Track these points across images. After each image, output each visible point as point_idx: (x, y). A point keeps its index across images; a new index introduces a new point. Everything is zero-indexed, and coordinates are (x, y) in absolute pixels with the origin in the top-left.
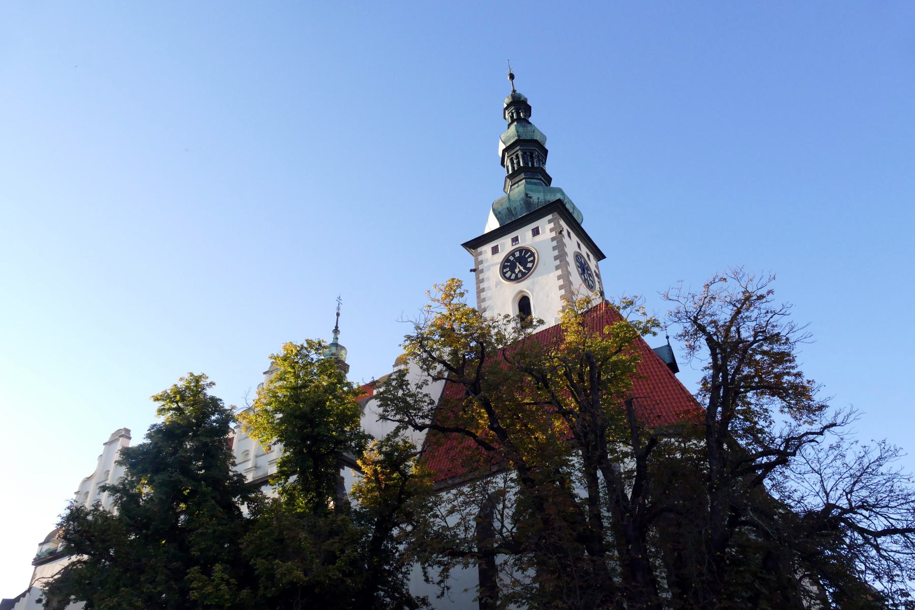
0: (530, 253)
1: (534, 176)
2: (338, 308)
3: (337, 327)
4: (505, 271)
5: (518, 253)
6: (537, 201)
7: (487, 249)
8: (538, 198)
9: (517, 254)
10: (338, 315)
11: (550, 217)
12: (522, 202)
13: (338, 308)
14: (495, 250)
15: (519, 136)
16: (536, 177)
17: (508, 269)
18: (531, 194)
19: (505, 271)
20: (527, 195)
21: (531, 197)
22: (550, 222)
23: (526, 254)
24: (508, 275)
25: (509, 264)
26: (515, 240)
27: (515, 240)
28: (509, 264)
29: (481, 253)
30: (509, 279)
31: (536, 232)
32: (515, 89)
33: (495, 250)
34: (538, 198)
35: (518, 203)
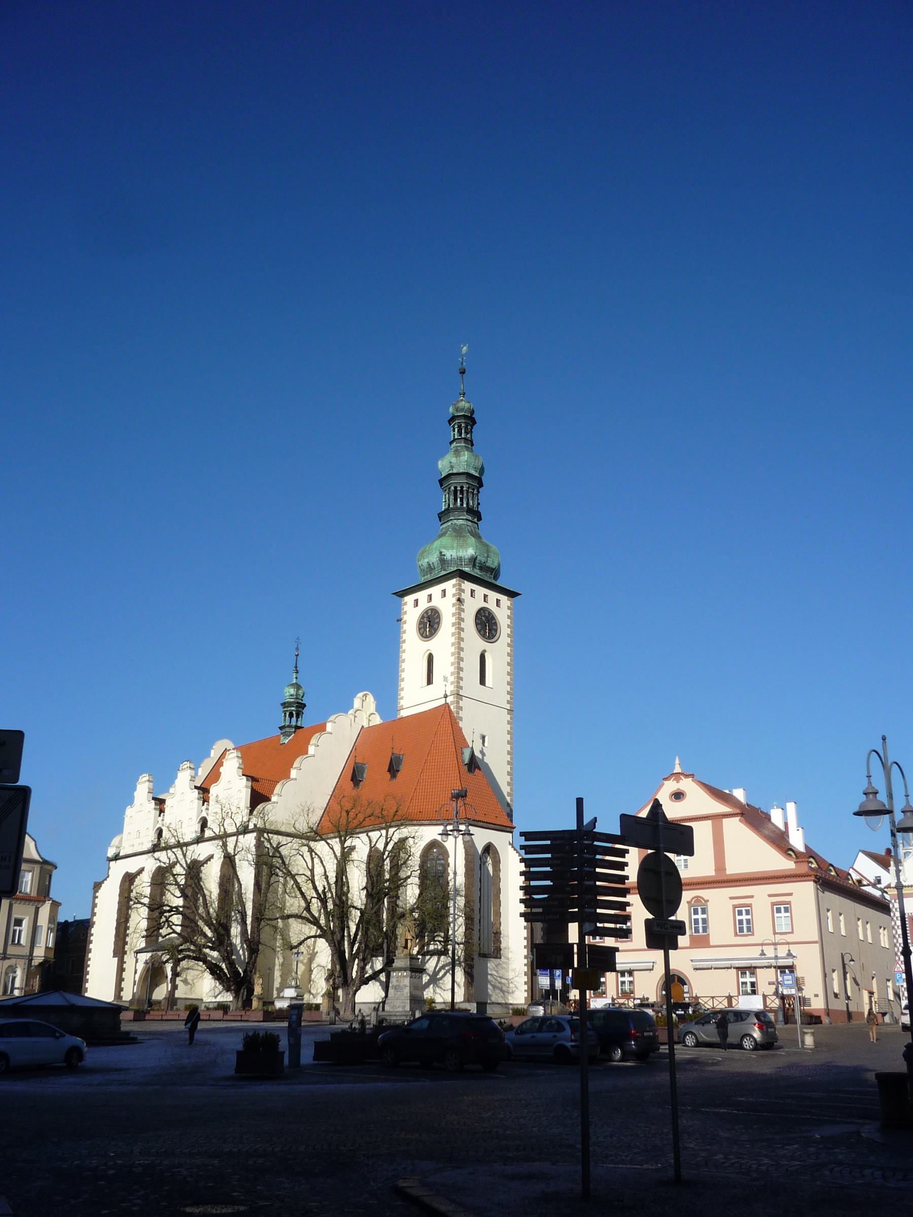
1: (461, 516)
2: (297, 649)
3: (296, 667)
6: (450, 558)
7: (409, 599)
8: (451, 556)
9: (430, 614)
10: (297, 655)
11: (454, 581)
12: (437, 559)
13: (297, 649)
15: (452, 467)
16: (461, 517)
18: (445, 552)
20: (441, 553)
21: (444, 555)
23: (434, 615)
33: (416, 602)
34: (451, 556)
35: (435, 560)
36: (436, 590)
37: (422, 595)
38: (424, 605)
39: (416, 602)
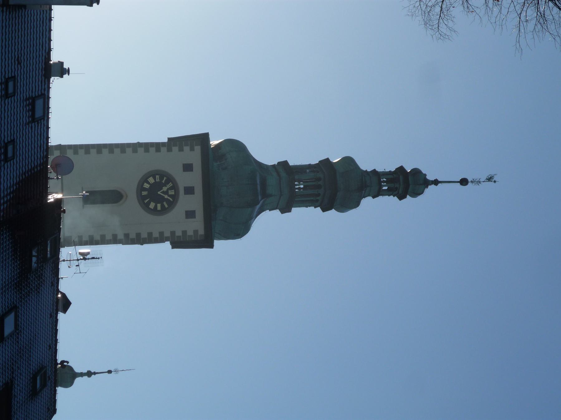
0: (166, 206)
4: (157, 177)
5: (173, 193)
9: (172, 192)
11: (201, 232)
14: (188, 168)
17: (158, 180)
19: (157, 177)
22: (196, 232)
24: (151, 180)
25: (163, 181)
26: (189, 191)
27: (189, 191)
28: (163, 181)
29: (192, 149)
30: (145, 179)
31: (190, 214)
32: (439, 184)
39: (188, 168)
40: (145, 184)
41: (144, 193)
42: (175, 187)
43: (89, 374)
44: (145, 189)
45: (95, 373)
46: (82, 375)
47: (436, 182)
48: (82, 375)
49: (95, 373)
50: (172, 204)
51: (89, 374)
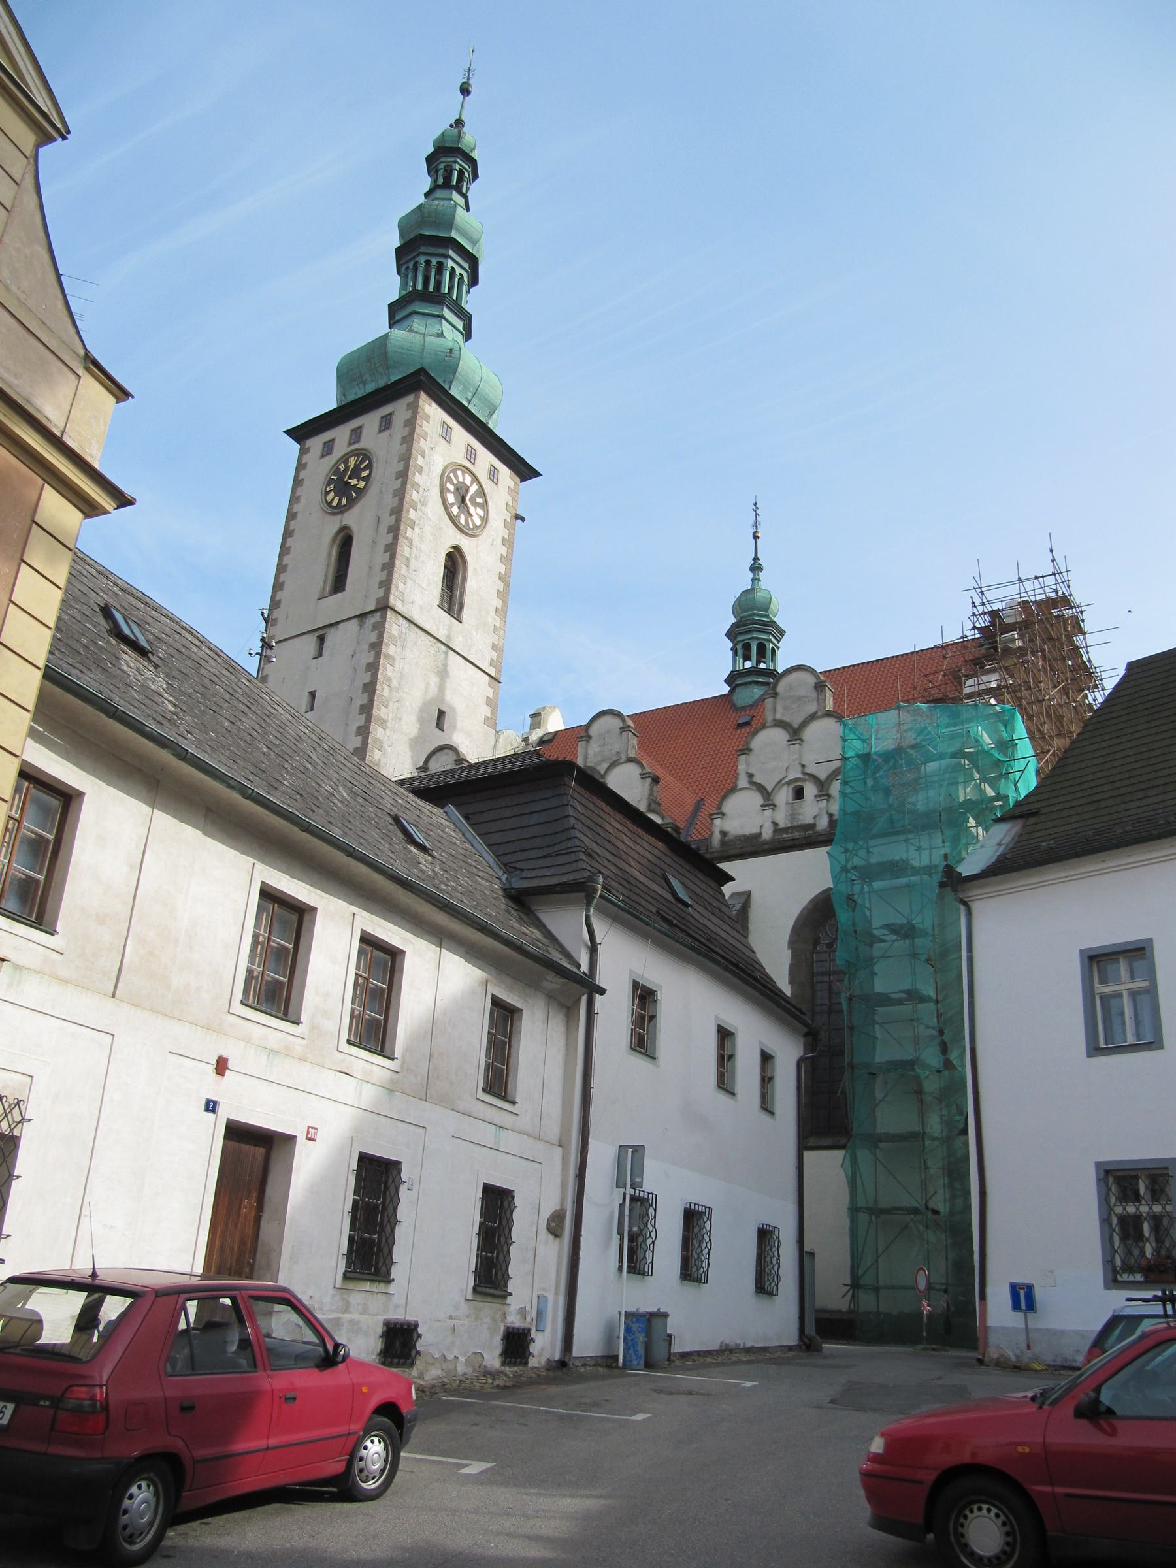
7: (316, 443)
17: (332, 487)
24: (329, 498)
26: (357, 434)
33: (328, 448)
36: (370, 422)
37: (341, 434)
38: (340, 449)
39: (328, 448)
40: (333, 504)
41: (344, 501)
42: (345, 460)
43: (756, 568)
44: (340, 501)
45: (756, 559)
46: (755, 580)
47: (459, 123)
48: (755, 580)
49: (756, 559)
50: (365, 456)
51: (756, 568)
